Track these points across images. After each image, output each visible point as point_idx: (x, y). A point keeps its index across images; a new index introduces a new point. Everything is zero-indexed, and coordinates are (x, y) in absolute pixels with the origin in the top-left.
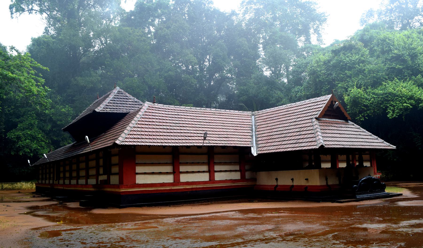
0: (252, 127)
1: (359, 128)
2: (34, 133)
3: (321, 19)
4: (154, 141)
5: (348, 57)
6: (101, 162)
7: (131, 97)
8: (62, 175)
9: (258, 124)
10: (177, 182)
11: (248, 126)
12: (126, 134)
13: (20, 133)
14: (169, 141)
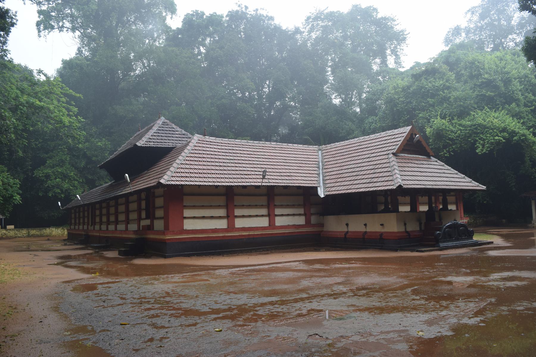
0: (319, 164)
1: (443, 166)
2: (66, 170)
3: (400, 38)
4: (205, 180)
5: (430, 82)
7: (179, 129)
8: (98, 219)
9: (325, 160)
10: (231, 227)
11: (314, 163)
12: (172, 172)
13: (49, 171)
14: (222, 180)
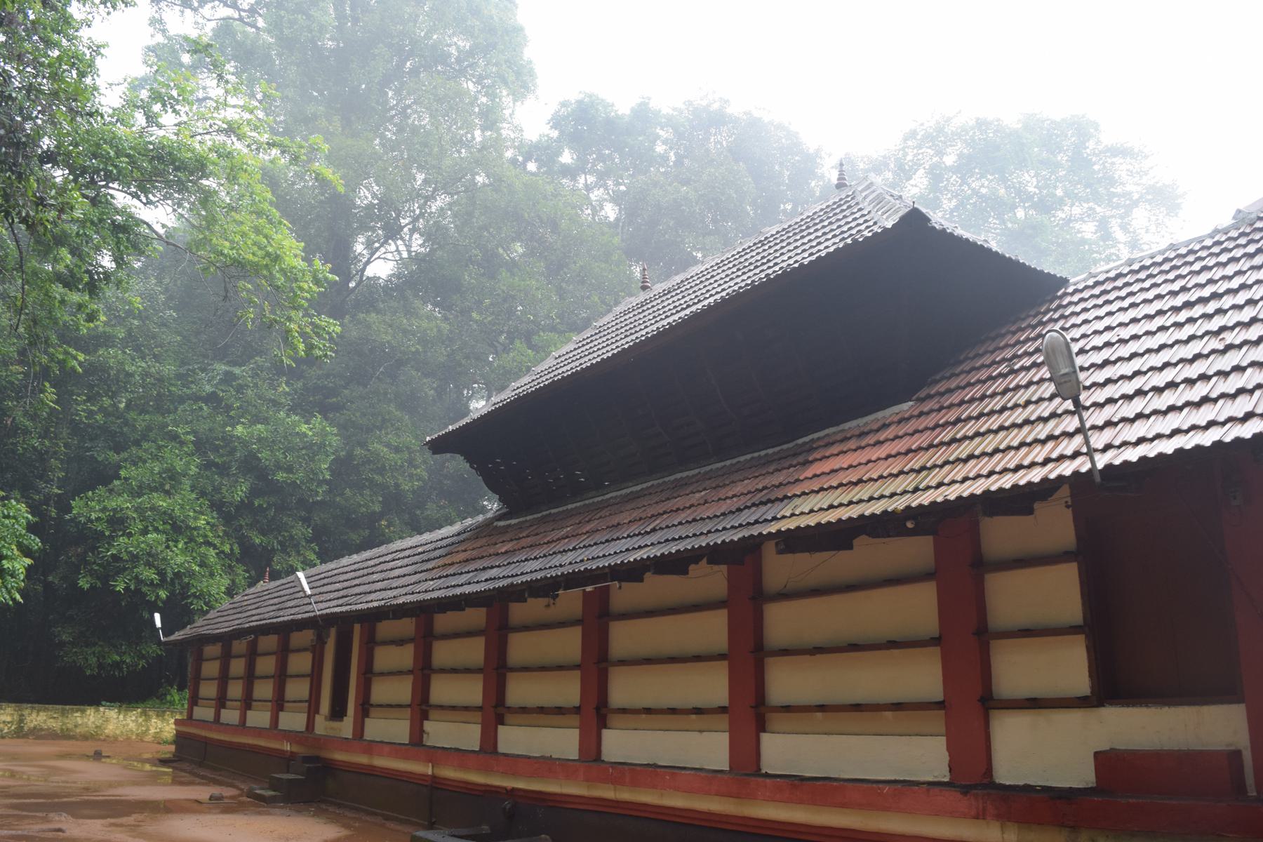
2: (182, 507)
13: (123, 502)
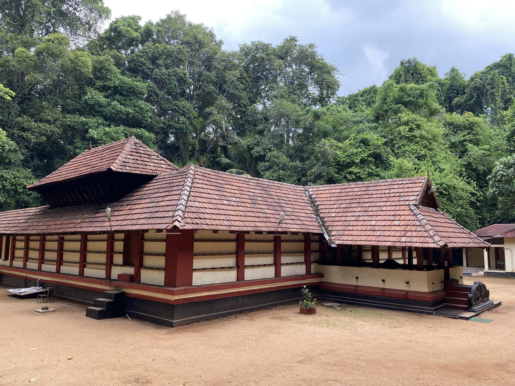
6: (119, 246)
8: (19, 253)
